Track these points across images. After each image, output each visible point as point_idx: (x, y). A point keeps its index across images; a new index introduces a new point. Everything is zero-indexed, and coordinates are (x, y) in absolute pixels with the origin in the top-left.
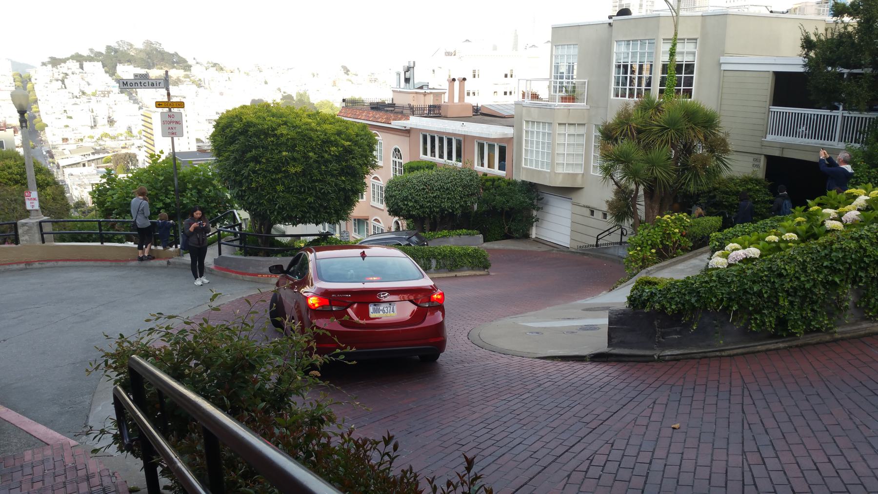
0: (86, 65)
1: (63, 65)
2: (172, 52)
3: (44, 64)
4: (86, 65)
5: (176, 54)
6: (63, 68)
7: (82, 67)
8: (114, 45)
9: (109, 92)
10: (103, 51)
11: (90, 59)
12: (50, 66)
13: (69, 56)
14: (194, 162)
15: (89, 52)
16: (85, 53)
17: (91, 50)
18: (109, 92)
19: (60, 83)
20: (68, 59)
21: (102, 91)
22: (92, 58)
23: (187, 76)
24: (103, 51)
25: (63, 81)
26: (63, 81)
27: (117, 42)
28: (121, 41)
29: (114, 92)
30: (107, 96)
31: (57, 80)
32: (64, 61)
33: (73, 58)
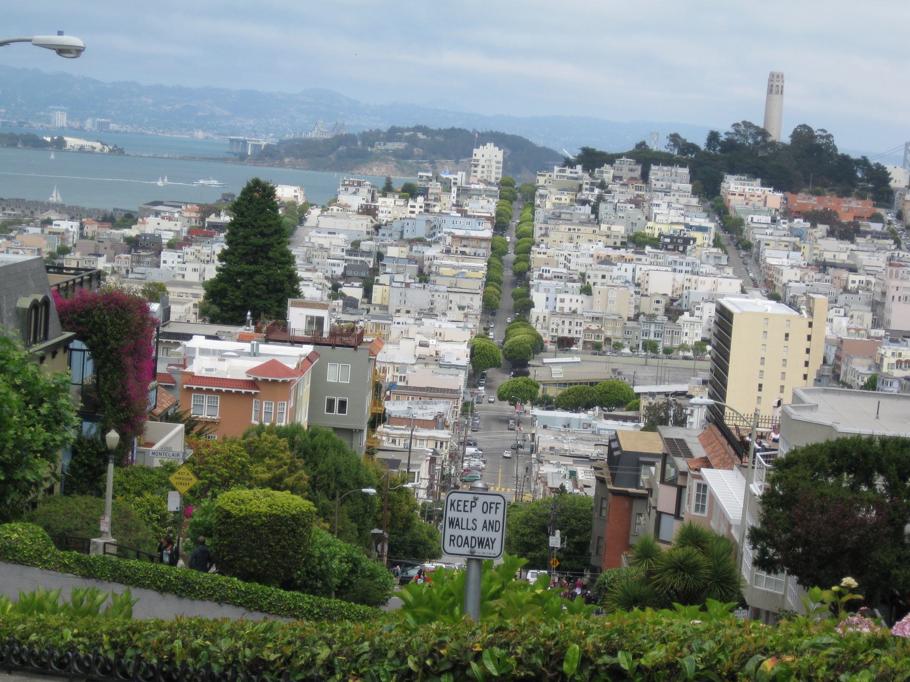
0: (656, 171)
1: (607, 167)
2: (855, 156)
3: (569, 163)
4: (656, 171)
5: (864, 162)
6: (607, 173)
7: (645, 177)
8: (724, 128)
9: (687, 241)
10: (703, 146)
11: (666, 160)
12: (579, 168)
13: (625, 151)
14: (642, 459)
15: (667, 141)
16: (660, 145)
17: (675, 138)
18: (687, 241)
19: (587, 209)
20: (619, 156)
21: (671, 237)
22: (672, 156)
23: (877, 218)
24: (702, 143)
25: (595, 210)
26: (595, 210)
27: (736, 125)
28: (744, 123)
29: (699, 242)
30: (681, 248)
31: (584, 202)
32: (610, 159)
33: (629, 155)
